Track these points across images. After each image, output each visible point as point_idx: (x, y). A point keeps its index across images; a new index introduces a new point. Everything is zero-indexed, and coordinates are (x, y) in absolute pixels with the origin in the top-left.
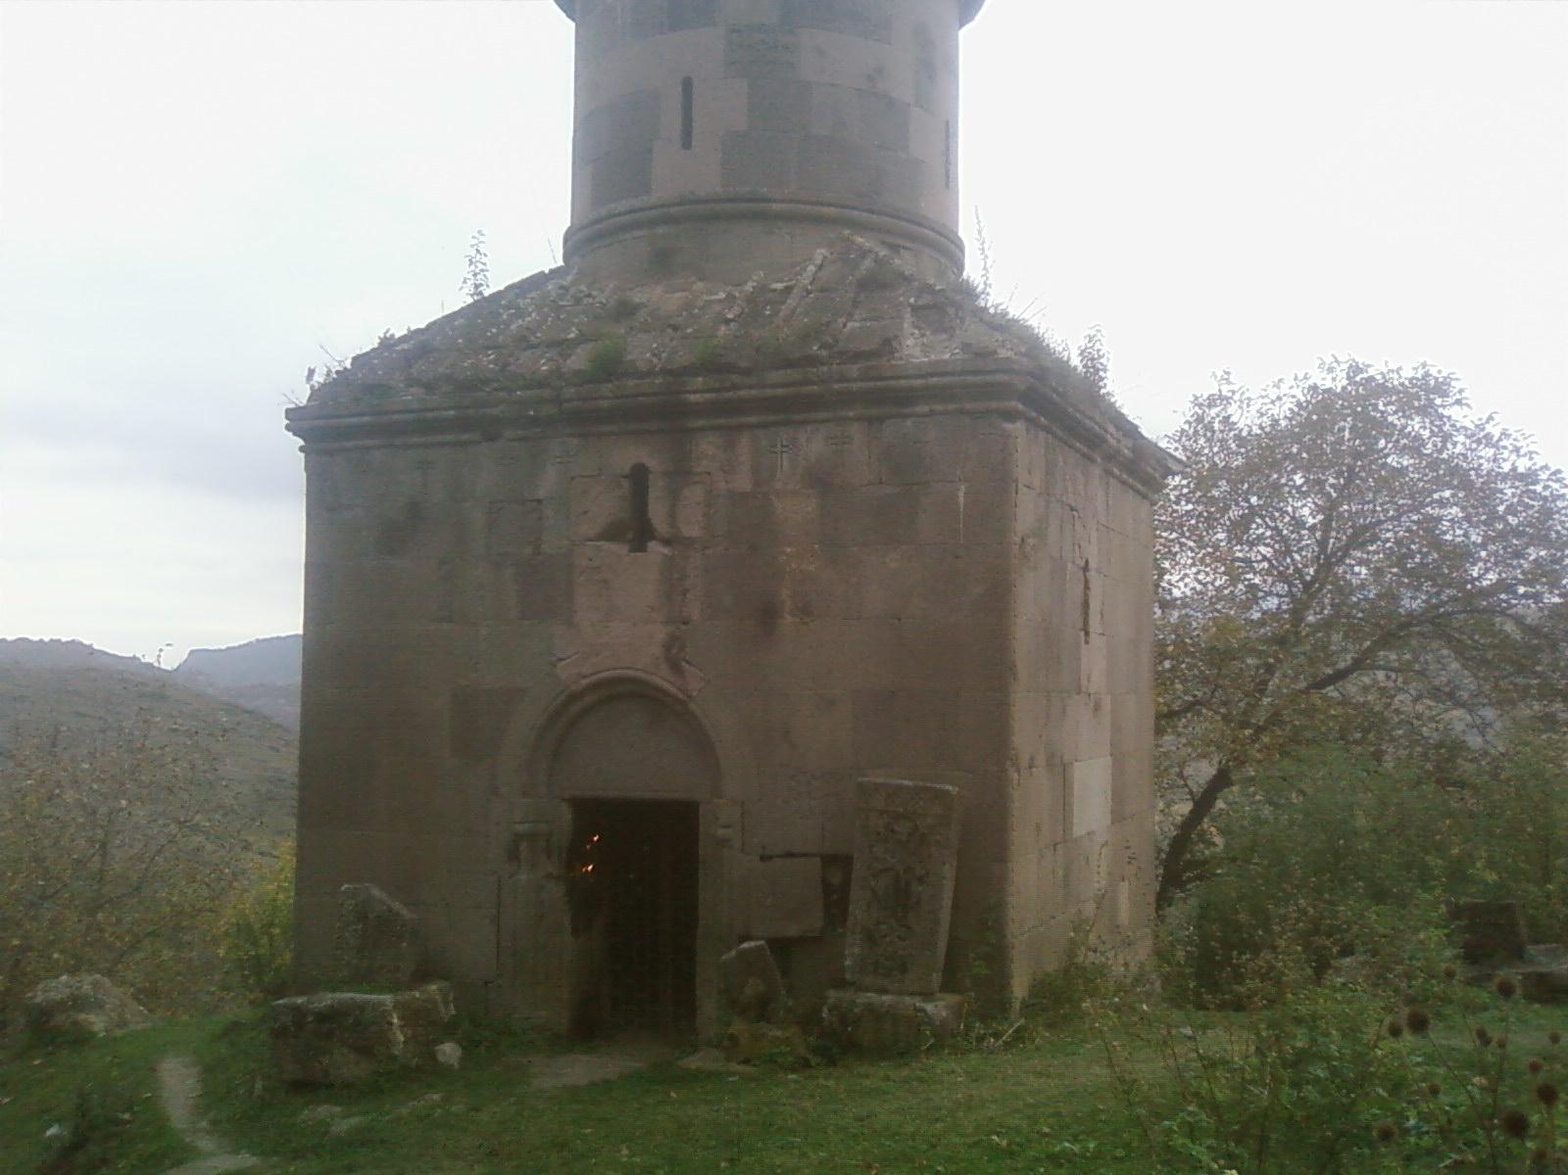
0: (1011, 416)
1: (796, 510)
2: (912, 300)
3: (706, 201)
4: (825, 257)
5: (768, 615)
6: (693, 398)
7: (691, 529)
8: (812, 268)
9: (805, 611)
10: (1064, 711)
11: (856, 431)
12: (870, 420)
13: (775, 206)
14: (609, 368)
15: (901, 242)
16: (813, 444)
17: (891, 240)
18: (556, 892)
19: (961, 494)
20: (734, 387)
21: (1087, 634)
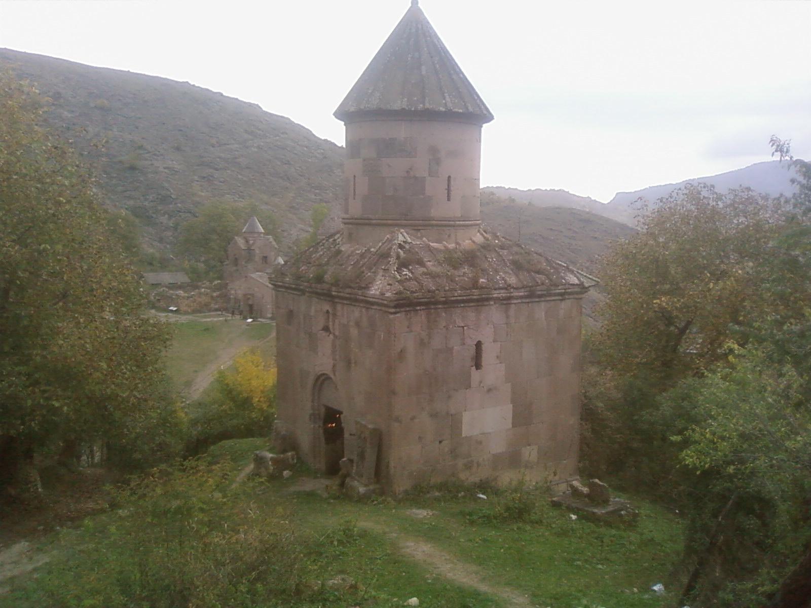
0: (395, 313)
1: (354, 332)
2: (383, 267)
3: (356, 219)
4: (388, 238)
5: (349, 363)
6: (334, 293)
7: (337, 333)
8: (380, 244)
9: (355, 363)
10: (449, 397)
11: (364, 310)
12: (368, 308)
13: (374, 222)
14: (319, 279)
15: (420, 228)
16: (356, 312)
17: (416, 228)
18: (321, 431)
19: (382, 336)
20: (340, 292)
21: (478, 366)
